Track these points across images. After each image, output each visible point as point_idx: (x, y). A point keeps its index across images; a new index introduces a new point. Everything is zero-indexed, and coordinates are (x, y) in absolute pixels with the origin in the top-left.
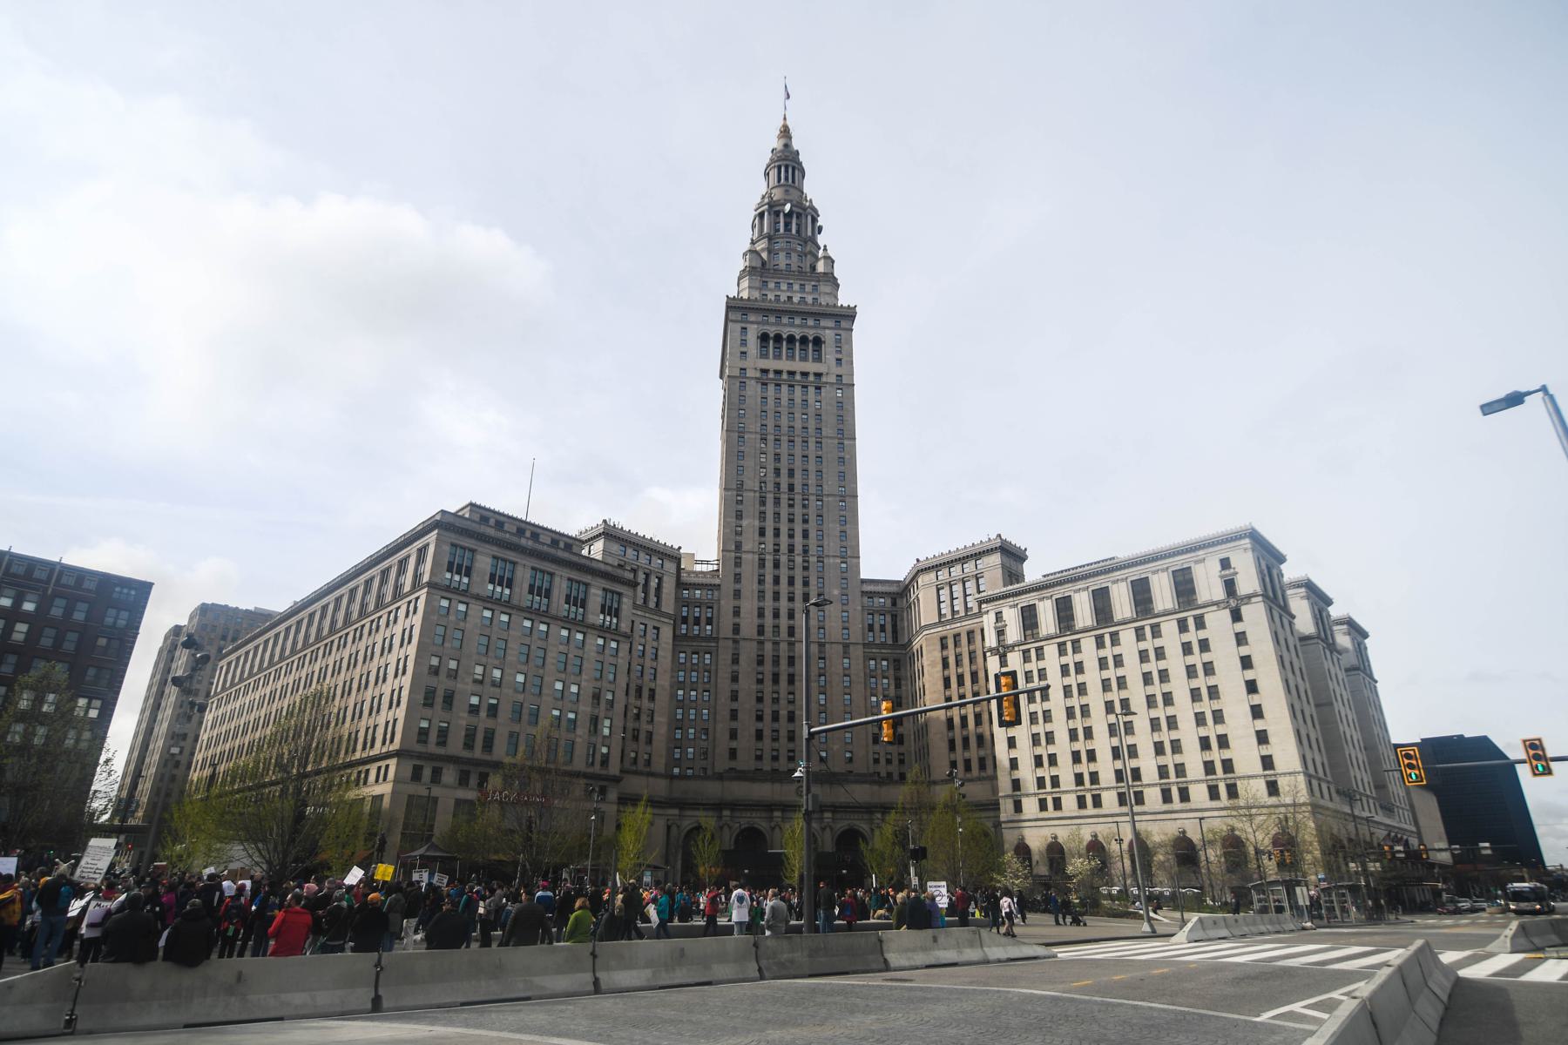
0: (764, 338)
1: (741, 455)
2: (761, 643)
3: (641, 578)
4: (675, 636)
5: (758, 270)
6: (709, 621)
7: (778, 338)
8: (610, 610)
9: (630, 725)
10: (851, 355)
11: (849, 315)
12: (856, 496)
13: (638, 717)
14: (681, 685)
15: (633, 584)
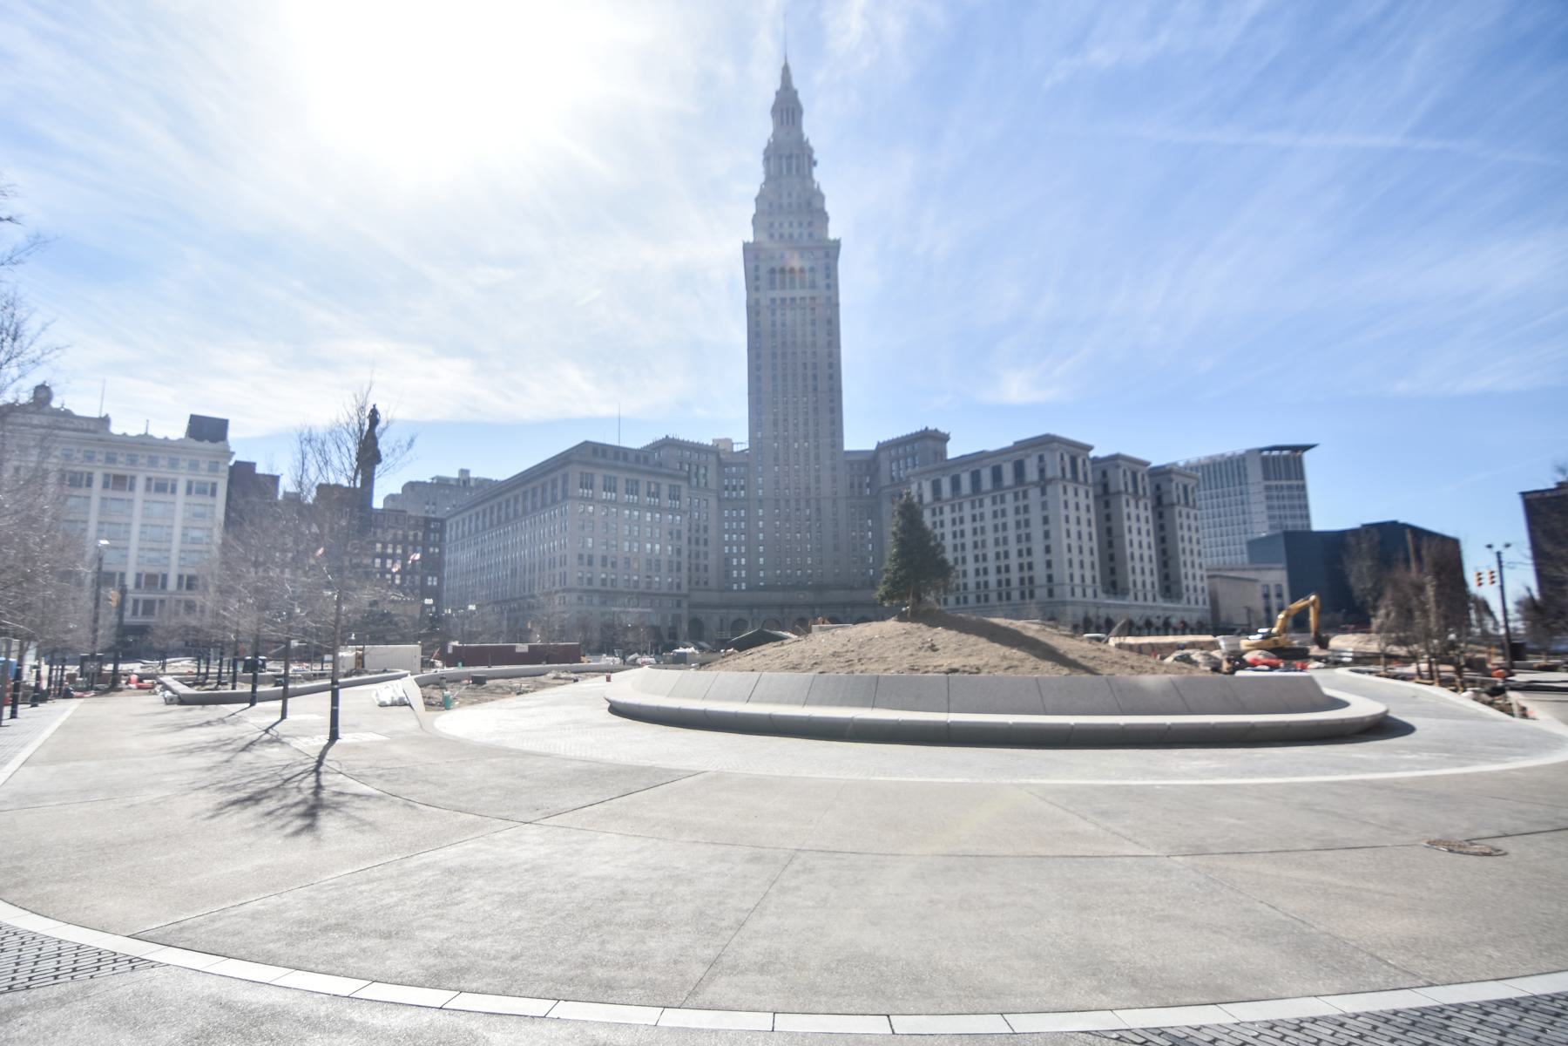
0: (772, 271)
1: (758, 368)
2: (777, 501)
3: (694, 468)
4: (719, 500)
5: (768, 210)
6: (742, 488)
7: (783, 271)
8: (674, 496)
9: (694, 562)
10: (836, 279)
11: (836, 245)
12: (840, 391)
13: (698, 556)
14: (726, 531)
15: (688, 479)
